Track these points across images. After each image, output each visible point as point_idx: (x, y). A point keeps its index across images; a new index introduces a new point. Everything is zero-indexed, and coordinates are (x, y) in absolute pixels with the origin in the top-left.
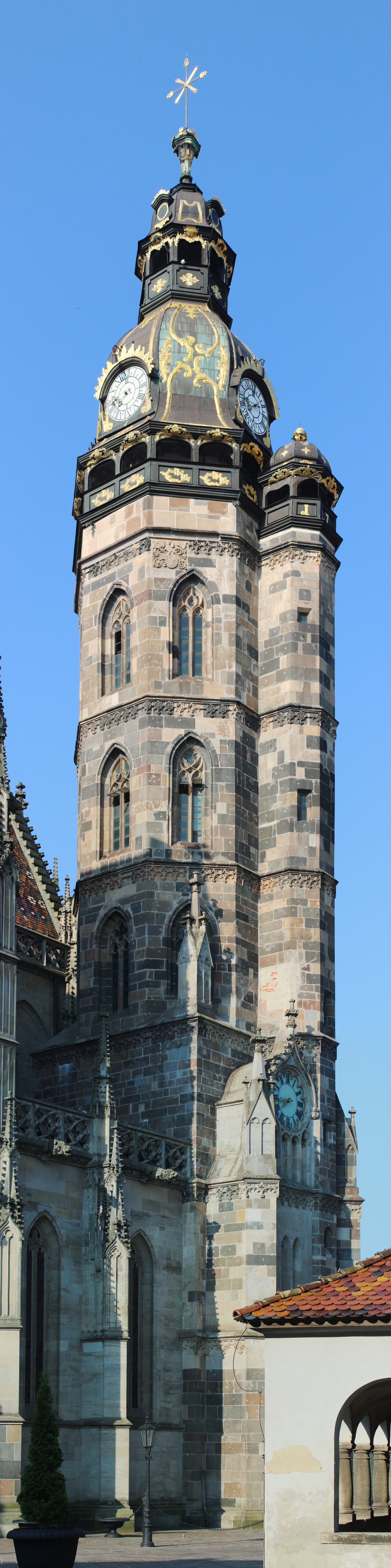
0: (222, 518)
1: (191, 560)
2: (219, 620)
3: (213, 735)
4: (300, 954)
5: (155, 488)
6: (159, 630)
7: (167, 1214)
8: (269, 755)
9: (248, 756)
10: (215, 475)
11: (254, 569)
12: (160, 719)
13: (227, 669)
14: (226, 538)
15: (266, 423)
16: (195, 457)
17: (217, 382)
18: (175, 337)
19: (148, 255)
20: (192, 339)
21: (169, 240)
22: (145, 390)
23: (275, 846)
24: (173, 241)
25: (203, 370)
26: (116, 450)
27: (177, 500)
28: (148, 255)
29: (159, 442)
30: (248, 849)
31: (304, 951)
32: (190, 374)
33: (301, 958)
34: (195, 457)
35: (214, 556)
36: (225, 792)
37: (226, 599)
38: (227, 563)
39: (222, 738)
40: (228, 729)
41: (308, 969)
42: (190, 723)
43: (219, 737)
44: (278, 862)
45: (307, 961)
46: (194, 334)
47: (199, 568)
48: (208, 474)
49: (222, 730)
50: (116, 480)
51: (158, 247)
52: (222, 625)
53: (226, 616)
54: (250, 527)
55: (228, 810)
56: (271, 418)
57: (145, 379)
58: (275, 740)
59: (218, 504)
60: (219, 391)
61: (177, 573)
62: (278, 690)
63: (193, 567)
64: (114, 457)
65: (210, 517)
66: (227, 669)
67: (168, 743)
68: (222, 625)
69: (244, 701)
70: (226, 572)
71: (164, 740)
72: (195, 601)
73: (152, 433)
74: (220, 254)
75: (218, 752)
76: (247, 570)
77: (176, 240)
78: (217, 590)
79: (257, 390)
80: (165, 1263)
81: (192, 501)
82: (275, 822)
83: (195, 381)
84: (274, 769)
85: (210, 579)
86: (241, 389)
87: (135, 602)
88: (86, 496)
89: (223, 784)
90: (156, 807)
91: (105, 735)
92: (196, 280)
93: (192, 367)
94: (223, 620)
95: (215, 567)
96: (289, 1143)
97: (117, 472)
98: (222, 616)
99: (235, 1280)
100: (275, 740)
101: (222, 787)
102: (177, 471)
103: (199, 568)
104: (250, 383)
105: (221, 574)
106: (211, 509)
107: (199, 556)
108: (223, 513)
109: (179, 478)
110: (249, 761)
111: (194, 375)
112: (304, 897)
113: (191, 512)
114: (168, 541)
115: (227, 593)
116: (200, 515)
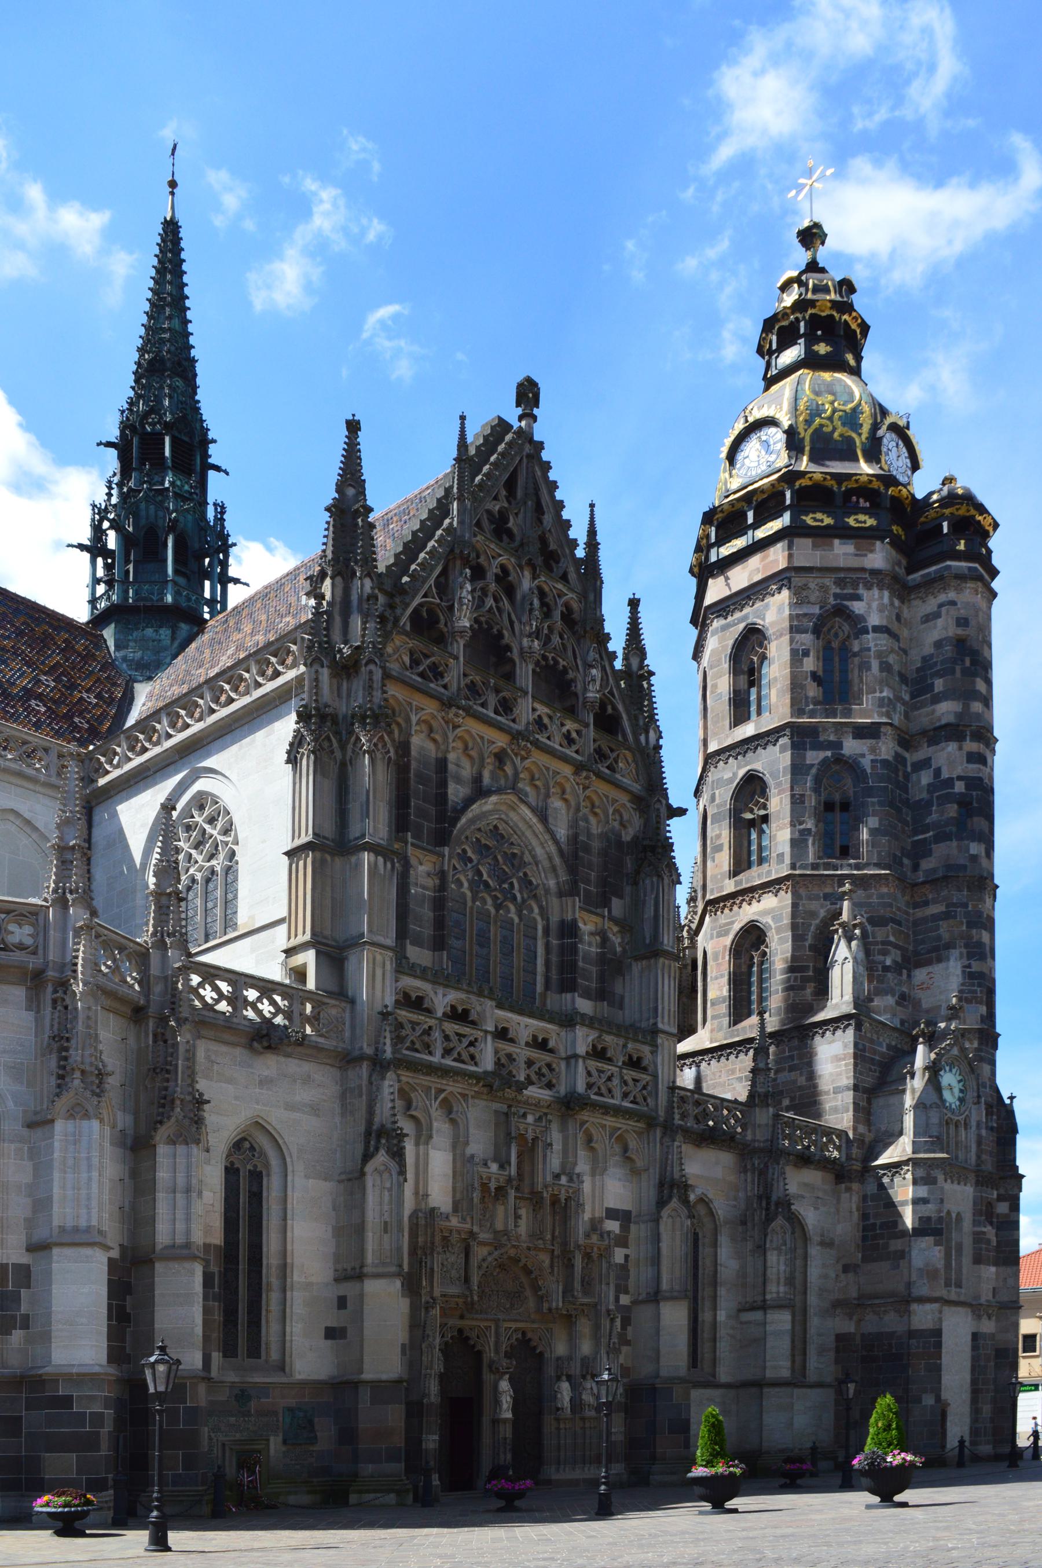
0: (870, 556)
1: (836, 596)
2: (869, 649)
3: (863, 756)
4: (961, 954)
8: (923, 772)
9: (901, 774)
11: (903, 602)
13: (878, 694)
14: (874, 572)
15: (909, 472)
17: (860, 435)
18: (812, 396)
20: (830, 398)
23: (930, 856)
25: (844, 424)
27: (819, 540)
31: (964, 951)
32: (830, 429)
33: (961, 957)
35: (861, 591)
36: (877, 808)
37: (876, 629)
38: (876, 597)
39: (872, 757)
40: (880, 749)
41: (969, 966)
44: (934, 870)
45: (969, 959)
46: (833, 394)
47: (845, 603)
48: (853, 517)
49: (873, 750)
52: (872, 653)
53: (876, 645)
54: (899, 564)
55: (880, 824)
56: (915, 466)
58: (930, 758)
59: (864, 542)
60: (862, 443)
61: (821, 608)
62: (933, 712)
63: (838, 601)
65: (856, 555)
66: (878, 694)
68: (872, 653)
69: (896, 722)
70: (875, 605)
72: (841, 634)
75: (869, 771)
76: (897, 603)
78: (866, 621)
79: (900, 443)
81: (836, 542)
82: (931, 833)
83: (836, 435)
84: (929, 785)
85: (857, 612)
86: (885, 441)
89: (875, 800)
93: (832, 422)
94: (873, 649)
95: (862, 600)
96: (952, 1128)
98: (872, 645)
99: (896, 1252)
100: (930, 758)
101: (873, 804)
102: (819, 516)
103: (845, 603)
104: (894, 436)
105: (870, 607)
106: (857, 548)
107: (845, 591)
108: (872, 551)
109: (822, 521)
110: (901, 779)
111: (834, 429)
112: (965, 900)
113: (836, 551)
114: (811, 580)
115: (877, 623)
116: (844, 554)
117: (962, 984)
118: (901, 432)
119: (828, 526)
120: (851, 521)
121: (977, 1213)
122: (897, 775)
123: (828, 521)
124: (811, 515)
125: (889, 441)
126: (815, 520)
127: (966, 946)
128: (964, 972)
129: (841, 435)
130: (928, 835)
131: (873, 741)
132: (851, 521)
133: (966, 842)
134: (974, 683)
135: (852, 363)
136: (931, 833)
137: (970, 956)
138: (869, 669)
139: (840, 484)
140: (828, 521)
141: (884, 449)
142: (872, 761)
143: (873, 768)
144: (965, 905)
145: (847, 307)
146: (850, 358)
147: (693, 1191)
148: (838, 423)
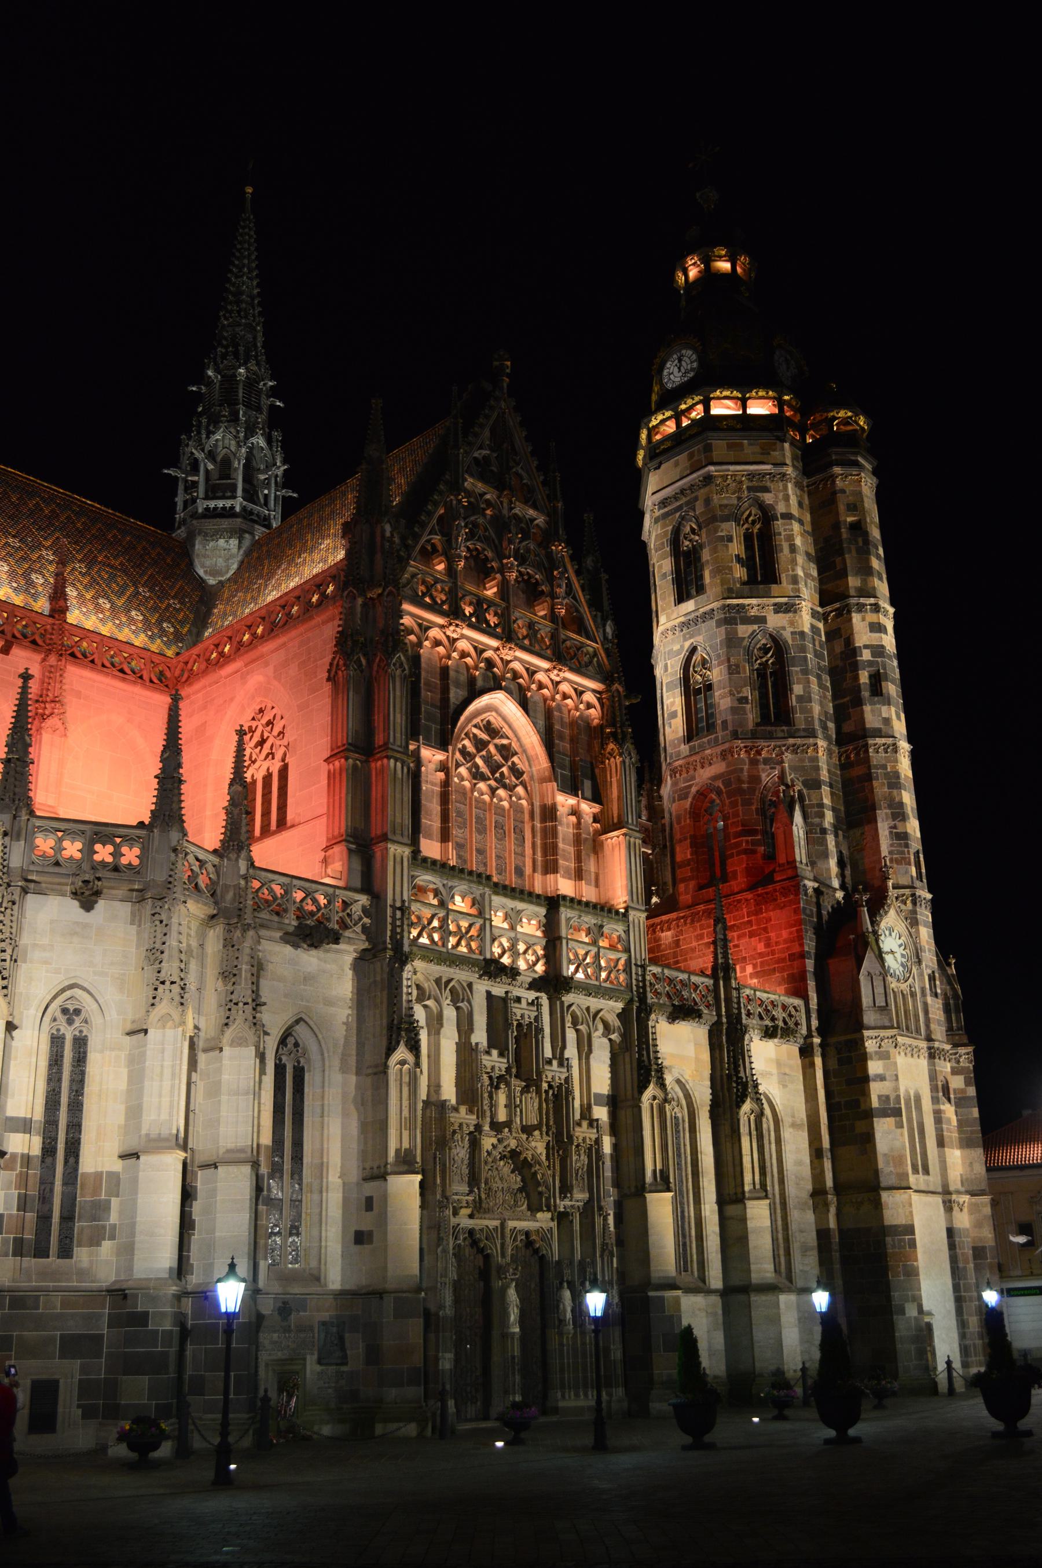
3: (784, 628)
6: (727, 546)
7: (787, 1071)
12: (735, 618)
30: (825, 724)
36: (800, 676)
39: (792, 630)
42: (761, 620)
43: (790, 630)
49: (792, 623)
67: (744, 638)
71: (740, 635)
75: (790, 642)
80: (790, 1120)
82: (848, 699)
84: (842, 653)
87: (703, 525)
89: (798, 669)
90: (739, 693)
91: (684, 636)
117: (892, 845)
121: (934, 1089)
122: (814, 645)
127: (890, 807)
128: (891, 833)
130: (845, 700)
131: (791, 615)
133: (878, 706)
134: (868, 561)
136: (848, 699)
137: (894, 816)
138: (781, 550)
142: (792, 633)
143: (793, 639)
144: (884, 767)
147: (670, 1072)
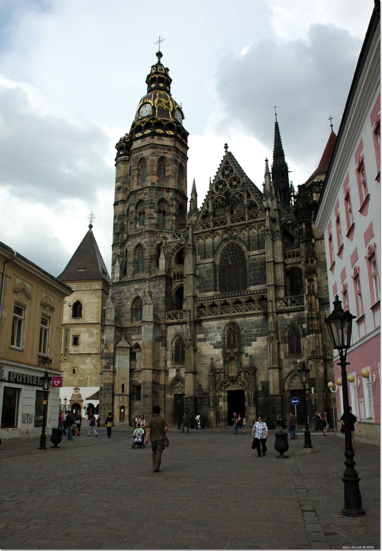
5: (153, 135)
10: (170, 132)
16: (165, 127)
19: (150, 78)
21: (156, 76)
22: (151, 110)
24: (157, 76)
25: (166, 105)
26: (143, 124)
28: (150, 78)
29: (155, 122)
34: (165, 127)
50: (143, 131)
51: (153, 77)
57: (151, 107)
64: (142, 125)
73: (153, 120)
74: (168, 80)
77: (158, 76)
83: (164, 108)
88: (134, 135)
92: (163, 85)
97: (143, 129)
109: (160, 131)
118: (180, 109)
119: (162, 133)
120: (167, 132)
123: (162, 132)
124: (158, 130)
125: (177, 112)
126: (159, 131)
129: (166, 108)
132: (167, 132)
135: (168, 89)
139: (165, 123)
140: (162, 132)
141: (176, 114)
145: (167, 75)
146: (168, 88)
148: (164, 106)
